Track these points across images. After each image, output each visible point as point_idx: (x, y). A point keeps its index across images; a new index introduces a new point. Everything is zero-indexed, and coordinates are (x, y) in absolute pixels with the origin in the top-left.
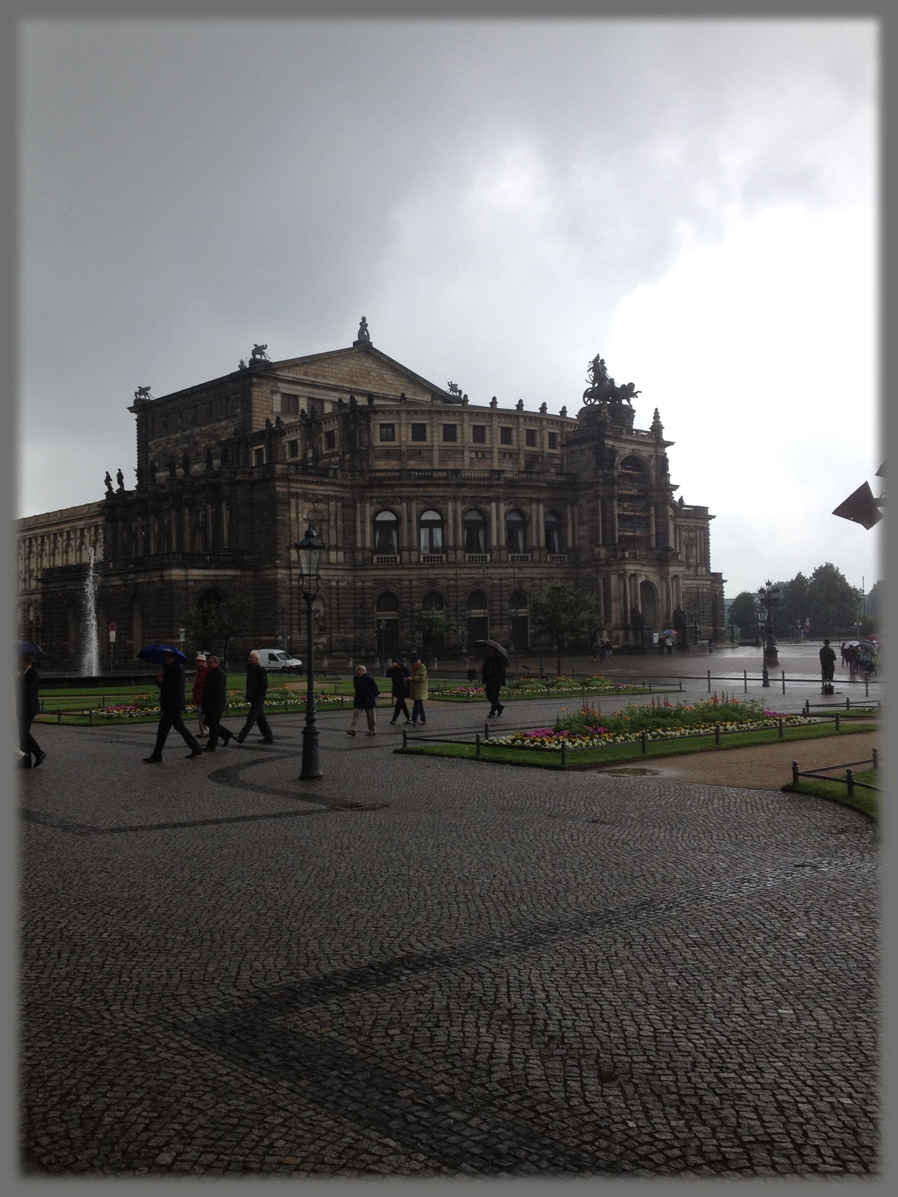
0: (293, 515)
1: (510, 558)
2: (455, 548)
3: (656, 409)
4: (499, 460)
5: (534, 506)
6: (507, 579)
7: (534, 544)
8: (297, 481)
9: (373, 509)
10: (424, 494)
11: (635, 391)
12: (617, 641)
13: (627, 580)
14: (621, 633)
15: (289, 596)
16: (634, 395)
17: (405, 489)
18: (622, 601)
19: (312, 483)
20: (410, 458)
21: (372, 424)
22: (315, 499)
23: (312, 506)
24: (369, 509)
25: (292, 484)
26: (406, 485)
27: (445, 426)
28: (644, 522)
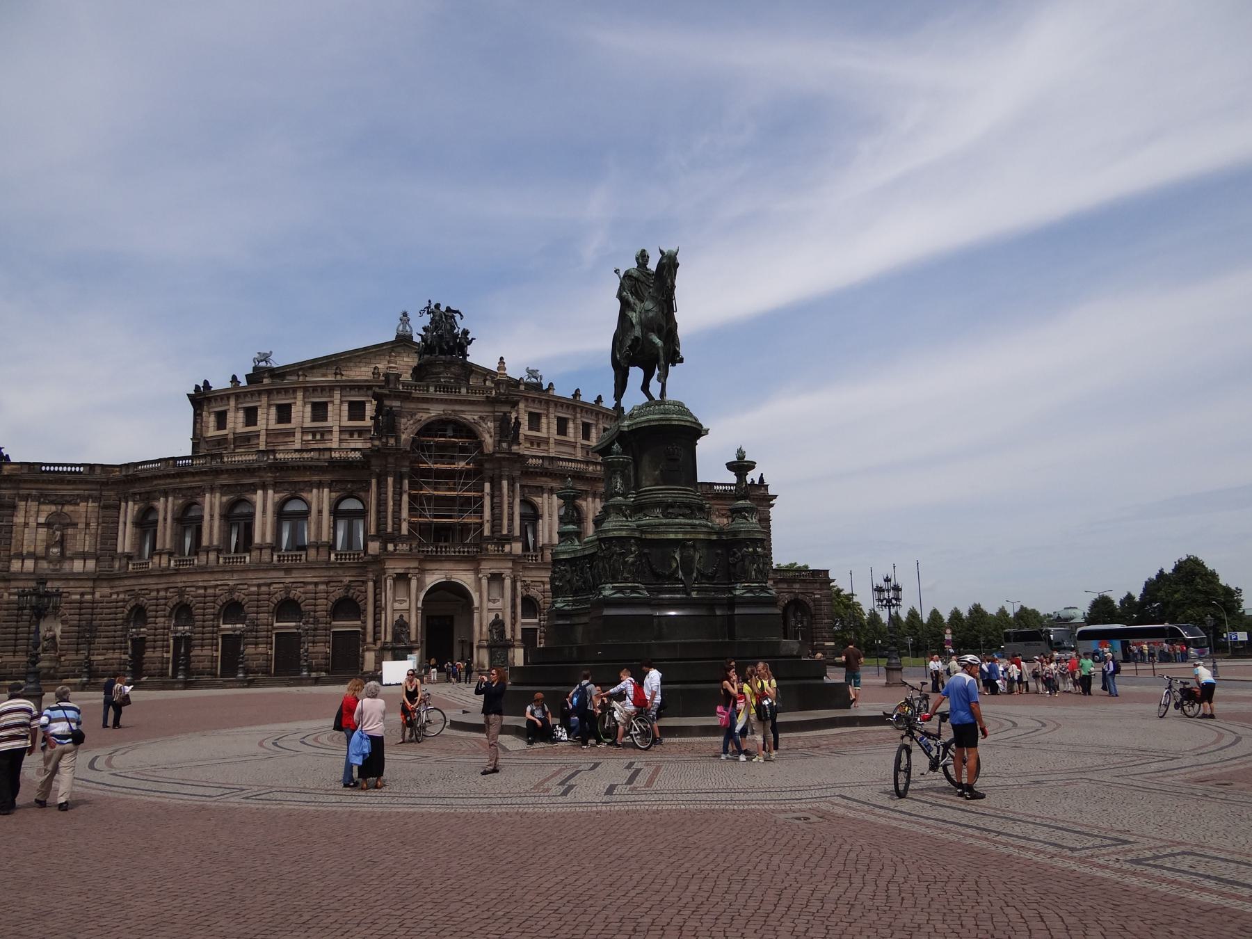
0: (19, 519)
1: (275, 558)
2: (208, 550)
3: (502, 358)
4: (341, 441)
5: (315, 491)
6: (269, 585)
8: (25, 481)
9: (136, 507)
10: (180, 486)
15: (5, 613)
16: (469, 343)
17: (162, 482)
19: (50, 482)
20: (236, 447)
22: (62, 501)
23: (53, 508)
24: (130, 510)
25: (22, 485)
26: (159, 477)
27: (279, 407)
28: (475, 505)
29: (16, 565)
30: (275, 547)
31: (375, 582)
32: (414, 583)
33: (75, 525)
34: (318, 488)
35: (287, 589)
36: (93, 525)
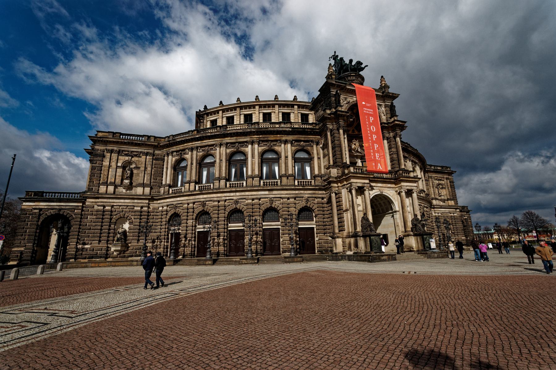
0: (106, 163)
3: (382, 77)
5: (283, 145)
7: (283, 172)
9: (174, 159)
11: (363, 66)
12: (350, 249)
13: (354, 192)
14: (352, 240)
15: (95, 217)
16: (362, 69)
18: (351, 210)
21: (205, 121)
22: (132, 154)
23: (127, 158)
24: (171, 160)
29: (103, 189)
30: (261, 178)
31: (336, 194)
32: (367, 193)
33: (137, 168)
34: (285, 144)
35: (272, 201)
36: (149, 169)
